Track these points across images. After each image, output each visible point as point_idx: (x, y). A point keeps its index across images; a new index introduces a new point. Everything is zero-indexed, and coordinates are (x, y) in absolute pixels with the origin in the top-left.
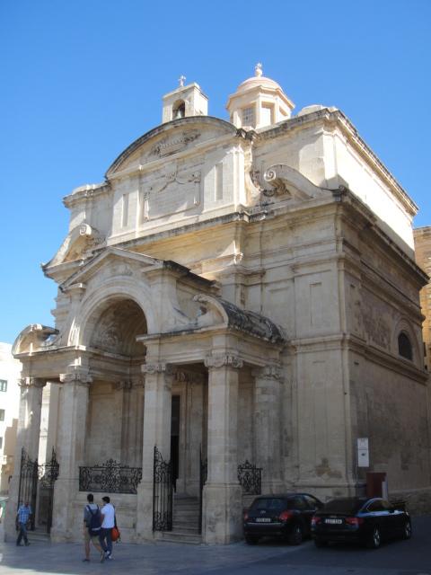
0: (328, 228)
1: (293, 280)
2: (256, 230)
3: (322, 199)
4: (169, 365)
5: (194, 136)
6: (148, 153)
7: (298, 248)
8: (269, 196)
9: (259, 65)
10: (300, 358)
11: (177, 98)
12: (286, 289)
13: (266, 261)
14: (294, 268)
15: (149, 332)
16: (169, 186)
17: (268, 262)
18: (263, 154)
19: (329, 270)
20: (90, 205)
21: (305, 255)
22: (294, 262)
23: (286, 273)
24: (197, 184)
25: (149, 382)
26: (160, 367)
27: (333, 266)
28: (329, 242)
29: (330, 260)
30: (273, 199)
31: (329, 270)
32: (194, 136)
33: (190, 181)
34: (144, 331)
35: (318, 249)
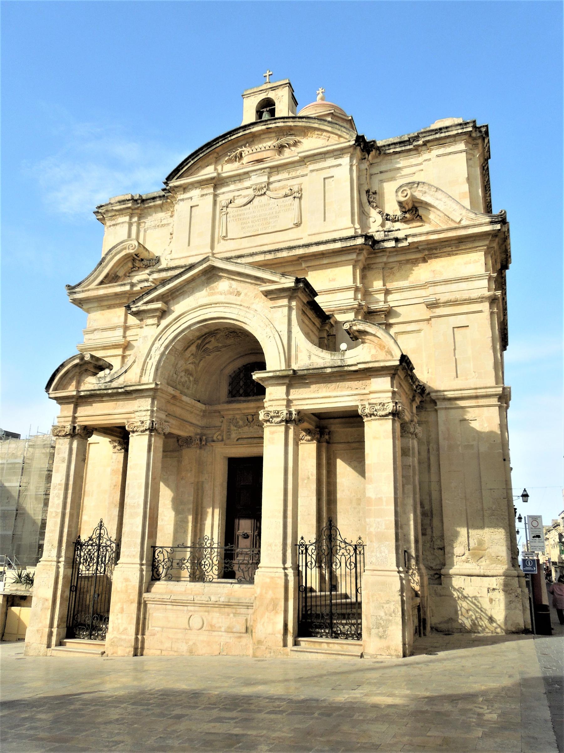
0: (476, 262)
1: (429, 320)
2: (378, 260)
3: (474, 226)
4: (299, 412)
5: (291, 142)
6: (227, 158)
7: (435, 283)
8: (394, 220)
9: (321, 90)
10: (442, 415)
11: (263, 96)
12: (419, 331)
13: (390, 298)
14: (432, 305)
15: (268, 368)
16: (257, 200)
17: (394, 300)
18: (381, 172)
19: (481, 311)
20: (135, 219)
21: (444, 293)
22: (432, 299)
23: (423, 312)
24: (297, 200)
25: (272, 433)
26: (290, 413)
27: (485, 306)
28: (479, 277)
29: (481, 300)
30: (398, 225)
31: (481, 311)
32: (291, 142)
33: (286, 196)
34: (262, 366)
35: (463, 285)
